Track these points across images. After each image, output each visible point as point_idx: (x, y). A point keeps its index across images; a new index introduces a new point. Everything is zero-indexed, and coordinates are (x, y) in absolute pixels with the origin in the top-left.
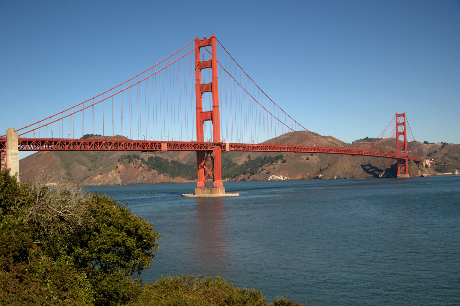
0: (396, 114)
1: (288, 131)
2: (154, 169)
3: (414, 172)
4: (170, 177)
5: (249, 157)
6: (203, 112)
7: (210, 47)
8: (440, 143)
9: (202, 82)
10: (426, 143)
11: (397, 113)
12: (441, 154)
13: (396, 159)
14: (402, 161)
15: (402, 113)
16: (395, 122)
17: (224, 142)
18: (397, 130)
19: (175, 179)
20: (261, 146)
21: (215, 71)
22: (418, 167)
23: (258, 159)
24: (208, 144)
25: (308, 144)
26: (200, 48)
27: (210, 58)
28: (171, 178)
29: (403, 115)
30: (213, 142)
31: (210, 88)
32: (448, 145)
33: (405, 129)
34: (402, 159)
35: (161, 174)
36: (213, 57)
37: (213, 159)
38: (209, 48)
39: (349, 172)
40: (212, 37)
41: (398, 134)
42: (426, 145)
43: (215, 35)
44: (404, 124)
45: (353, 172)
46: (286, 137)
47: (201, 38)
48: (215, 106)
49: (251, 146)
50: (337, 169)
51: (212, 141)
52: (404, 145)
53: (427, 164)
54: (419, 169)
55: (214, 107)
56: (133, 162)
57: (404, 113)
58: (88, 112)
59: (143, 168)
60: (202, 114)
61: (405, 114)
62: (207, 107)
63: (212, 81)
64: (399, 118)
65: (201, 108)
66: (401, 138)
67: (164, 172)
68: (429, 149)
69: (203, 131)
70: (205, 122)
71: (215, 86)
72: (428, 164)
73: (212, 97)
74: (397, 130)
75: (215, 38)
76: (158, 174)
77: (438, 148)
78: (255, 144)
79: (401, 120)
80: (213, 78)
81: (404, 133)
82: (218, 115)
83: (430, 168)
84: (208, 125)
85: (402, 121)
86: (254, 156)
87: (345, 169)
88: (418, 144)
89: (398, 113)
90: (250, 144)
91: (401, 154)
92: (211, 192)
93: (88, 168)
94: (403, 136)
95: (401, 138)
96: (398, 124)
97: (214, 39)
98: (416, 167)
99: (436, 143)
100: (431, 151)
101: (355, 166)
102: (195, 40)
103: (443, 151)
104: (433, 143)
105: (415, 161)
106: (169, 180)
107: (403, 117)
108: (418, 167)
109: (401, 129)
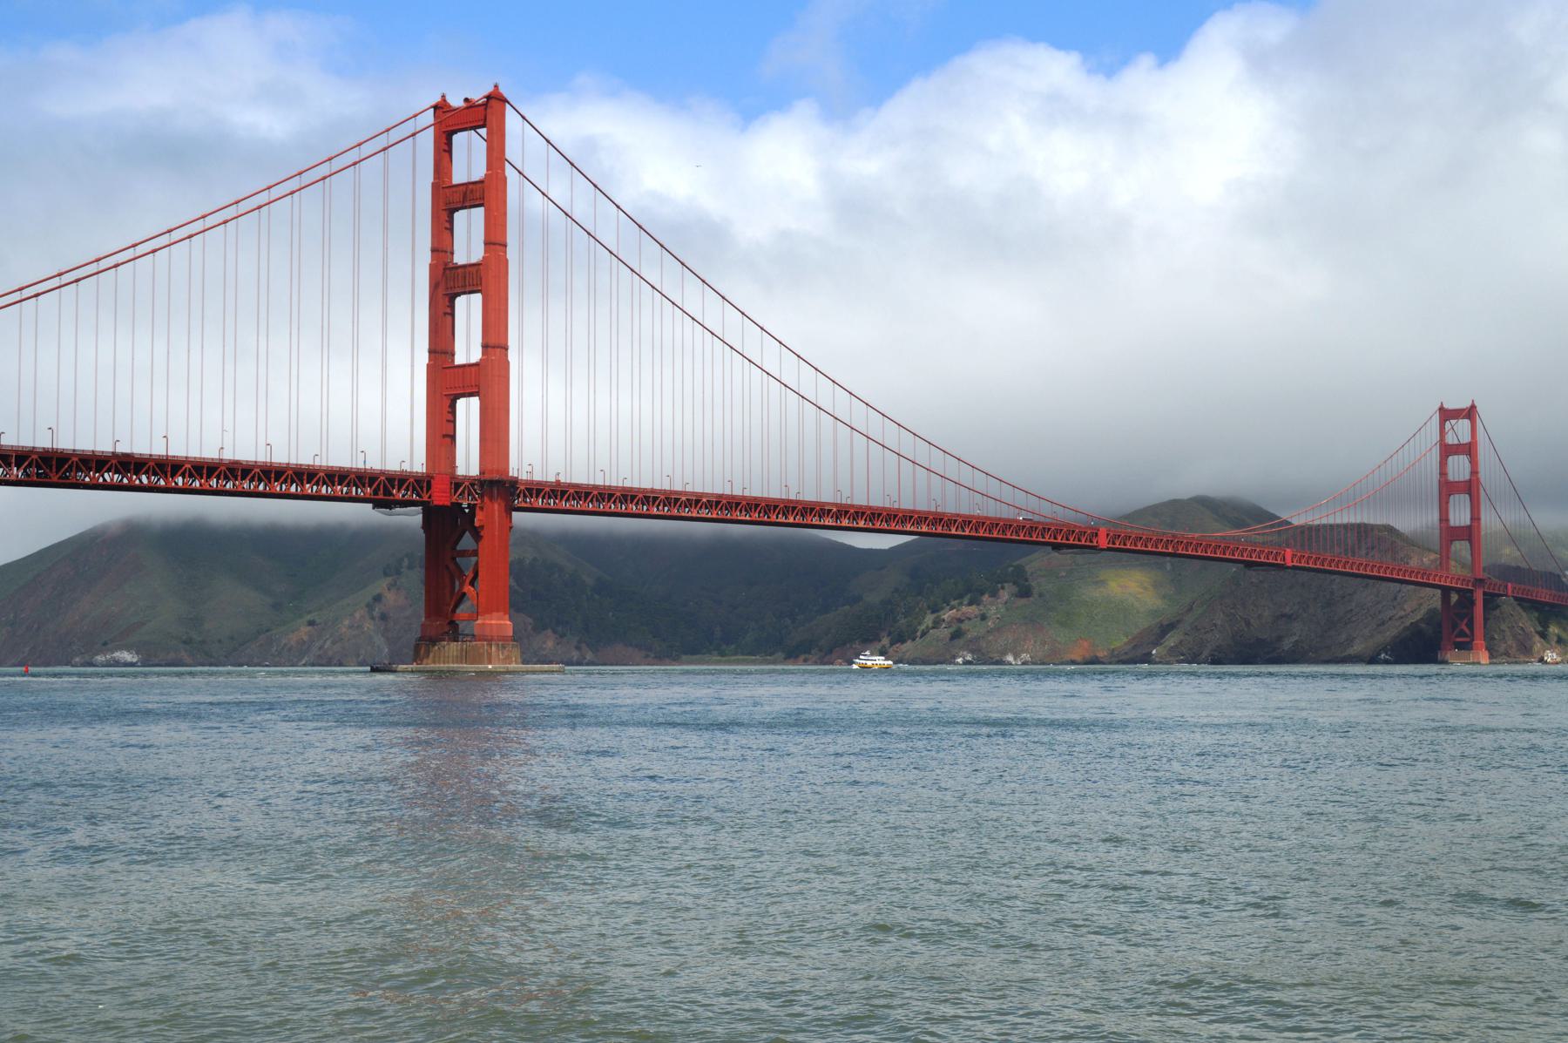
0: (1441, 409)
3: (1510, 642)
11: (1446, 406)
13: (1439, 592)
15: (1466, 404)
16: (1436, 437)
17: (524, 477)
18: (1443, 473)
20: (704, 500)
22: (1545, 625)
27: (479, 171)
29: (1470, 413)
33: (1474, 472)
34: (1458, 590)
35: (544, 628)
38: (483, 131)
40: (489, 97)
43: (502, 90)
44: (1469, 449)
47: (456, 101)
48: (495, 343)
49: (657, 498)
50: (1215, 625)
54: (1543, 635)
55: (485, 346)
57: (1473, 407)
69: (453, 437)
79: (1460, 431)
80: (488, 243)
84: (468, 411)
85: (1465, 438)
87: (1248, 624)
89: (1449, 406)
92: (465, 657)
94: (1467, 496)
96: (1447, 451)
102: (436, 107)
105: (1516, 599)
107: (1466, 422)
108: (1544, 624)
109: (1459, 468)
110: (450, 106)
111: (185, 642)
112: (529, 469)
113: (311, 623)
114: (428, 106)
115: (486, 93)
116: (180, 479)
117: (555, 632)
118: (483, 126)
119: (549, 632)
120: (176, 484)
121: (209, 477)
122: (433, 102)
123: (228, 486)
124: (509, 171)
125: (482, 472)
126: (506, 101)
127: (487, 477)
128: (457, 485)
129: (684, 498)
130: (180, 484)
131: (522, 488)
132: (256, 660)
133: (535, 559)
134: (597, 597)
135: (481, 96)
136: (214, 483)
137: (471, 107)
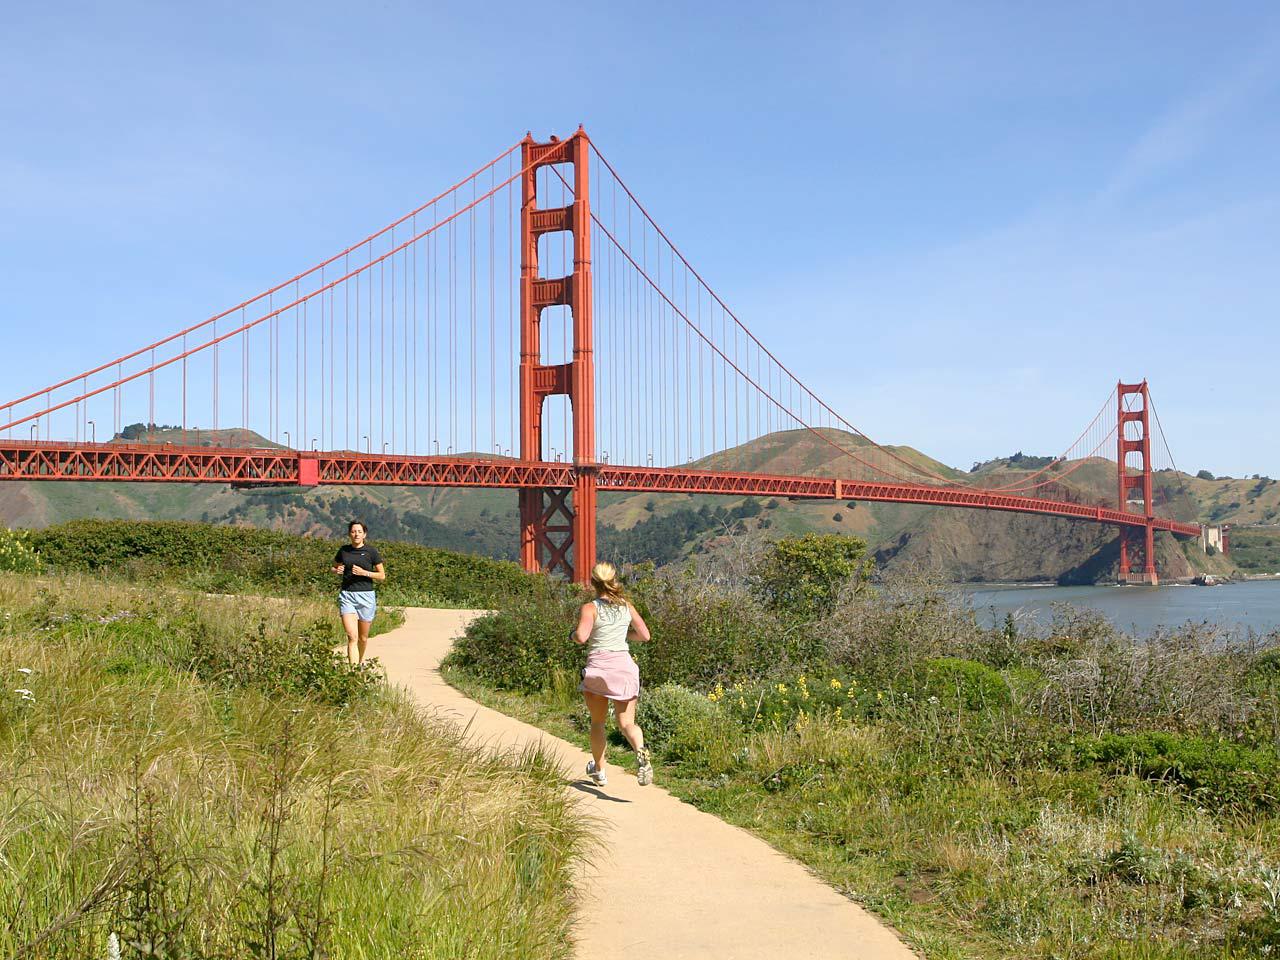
1: (789, 425)
5: (650, 508)
6: (545, 368)
7: (570, 166)
8: (1250, 477)
9: (542, 274)
10: (1203, 475)
11: (1124, 383)
12: (1252, 512)
14: (1135, 534)
18: (1121, 435)
23: (681, 514)
24: (558, 471)
25: (840, 471)
26: (535, 168)
27: (570, 200)
29: (1141, 388)
30: (570, 461)
31: (566, 292)
32: (1275, 485)
33: (1146, 434)
36: (577, 195)
39: (970, 561)
40: (577, 137)
41: (1125, 447)
42: (1205, 481)
43: (586, 130)
44: (1141, 416)
45: (980, 562)
46: (767, 446)
47: (541, 138)
48: (581, 349)
51: (568, 458)
52: (1138, 483)
53: (1213, 545)
55: (576, 352)
56: (283, 515)
57: (1145, 383)
58: (200, 363)
60: (538, 372)
61: (1148, 386)
62: (555, 351)
63: (575, 270)
64: (1129, 396)
65: (536, 355)
66: (1134, 460)
68: (1216, 496)
72: (1215, 543)
73: (570, 321)
74: (1121, 435)
75: (587, 139)
77: (1243, 493)
79: (1133, 402)
80: (576, 263)
81: (1142, 446)
82: (588, 377)
83: (1221, 558)
85: (1138, 407)
86: (669, 503)
87: (955, 552)
88: (1180, 477)
91: (1133, 507)
95: (1134, 460)
96: (1124, 417)
97: (582, 140)
98: (1179, 552)
99: (1236, 475)
100: (1221, 503)
101: (987, 545)
103: (1261, 503)
104: (1227, 478)
109: (1133, 430)
127: (581, 462)
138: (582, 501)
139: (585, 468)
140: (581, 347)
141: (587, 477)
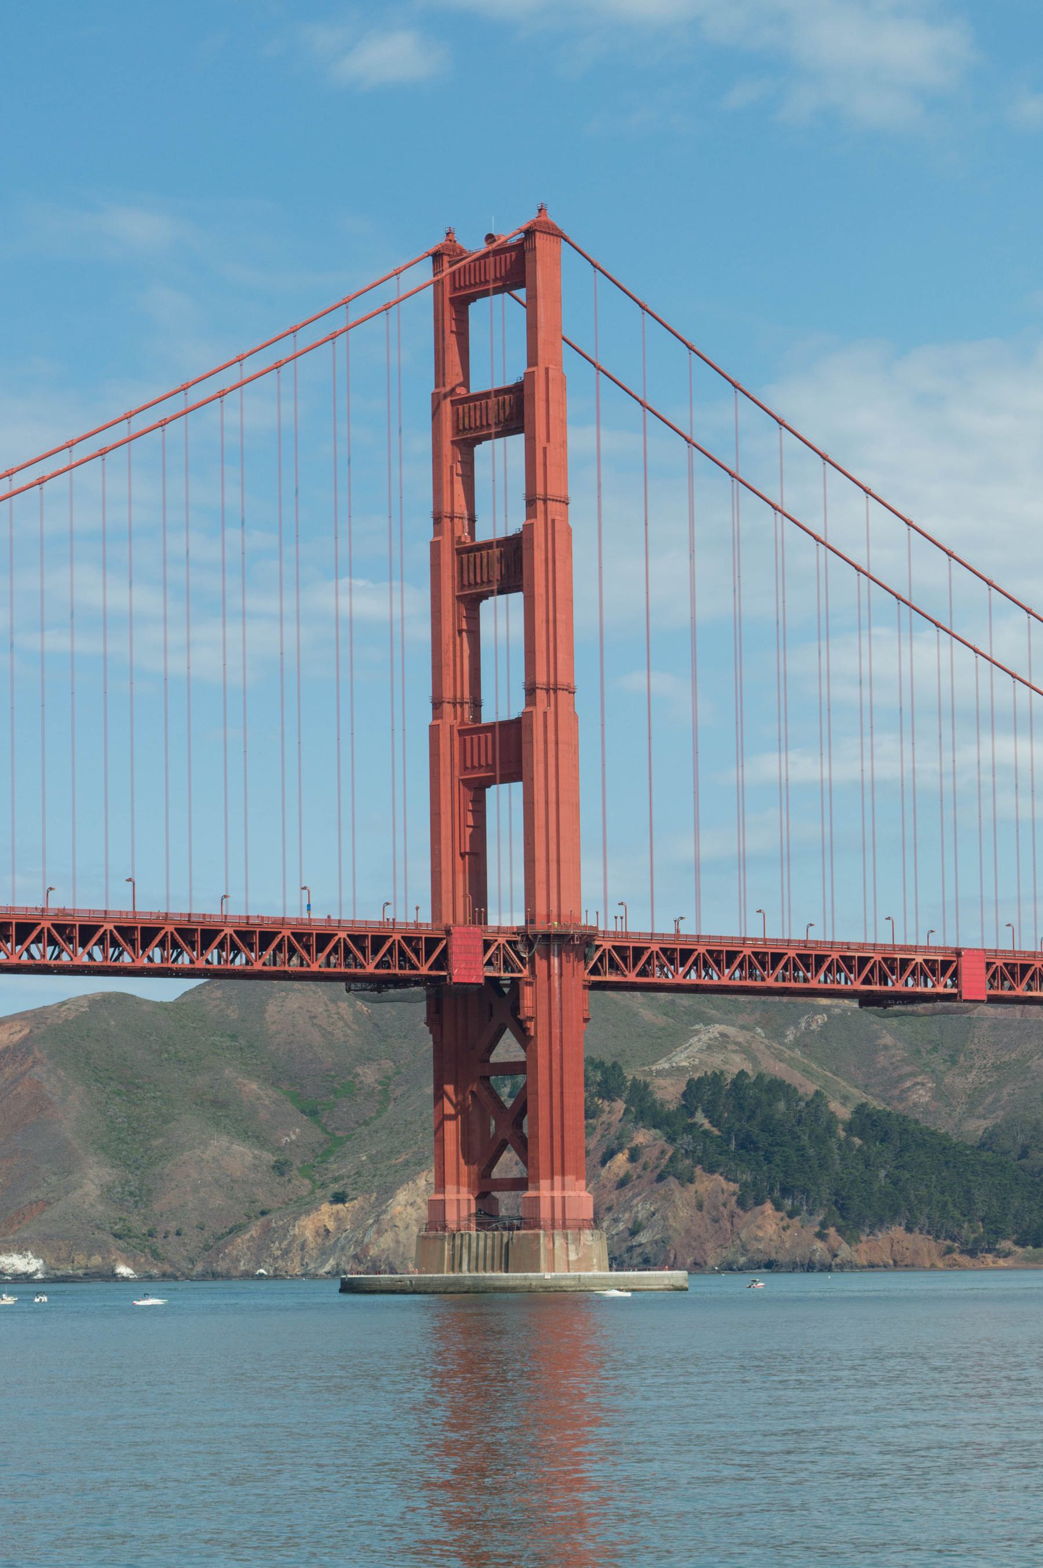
2: (711, 1170)
4: (824, 1225)
19: (863, 1247)
21: (545, 449)
27: (513, 372)
28: (832, 1231)
30: (519, 921)
35: (759, 1202)
37: (525, 1038)
40: (529, 233)
43: (554, 217)
47: (474, 244)
59: (633, 1158)
67: (786, 1191)
70: (491, 792)
71: (539, 556)
76: (741, 1203)
78: (904, 948)
90: (862, 947)
93: (270, 1158)
97: (541, 241)
106: (819, 1245)
110: (462, 251)
111: (117, 1236)
112: (620, 911)
113: (339, 1198)
114: (422, 254)
115: (524, 224)
116: (157, 951)
117: (778, 1207)
118: (522, 285)
119: (768, 1207)
120: (151, 960)
121: (205, 946)
122: (431, 248)
123: (238, 961)
124: (571, 364)
125: (530, 919)
126: (560, 236)
127: (540, 927)
128: (487, 945)
129: (919, 959)
130: (157, 959)
131: (607, 945)
132: (242, 1266)
133: (742, 1074)
134: (857, 1141)
135: (515, 231)
136: (213, 955)
137: (497, 252)
138: (543, 1008)
139: (547, 937)
140: (541, 679)
141: (555, 961)
